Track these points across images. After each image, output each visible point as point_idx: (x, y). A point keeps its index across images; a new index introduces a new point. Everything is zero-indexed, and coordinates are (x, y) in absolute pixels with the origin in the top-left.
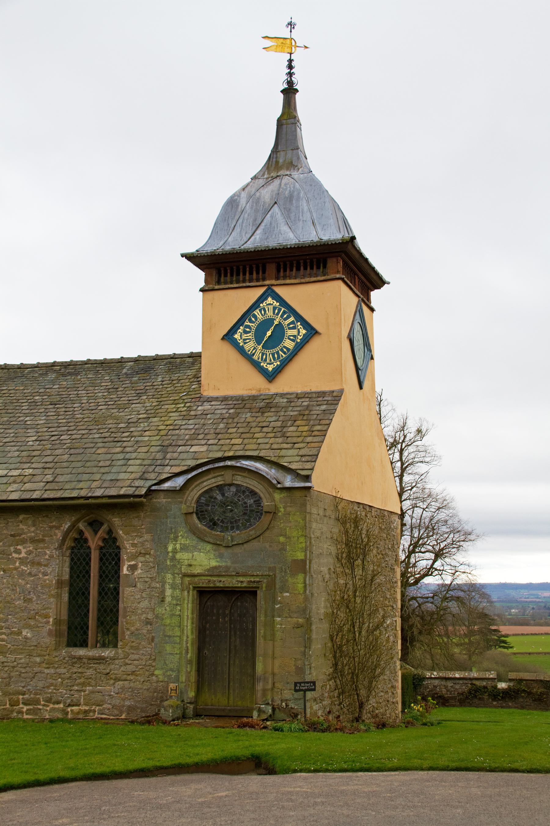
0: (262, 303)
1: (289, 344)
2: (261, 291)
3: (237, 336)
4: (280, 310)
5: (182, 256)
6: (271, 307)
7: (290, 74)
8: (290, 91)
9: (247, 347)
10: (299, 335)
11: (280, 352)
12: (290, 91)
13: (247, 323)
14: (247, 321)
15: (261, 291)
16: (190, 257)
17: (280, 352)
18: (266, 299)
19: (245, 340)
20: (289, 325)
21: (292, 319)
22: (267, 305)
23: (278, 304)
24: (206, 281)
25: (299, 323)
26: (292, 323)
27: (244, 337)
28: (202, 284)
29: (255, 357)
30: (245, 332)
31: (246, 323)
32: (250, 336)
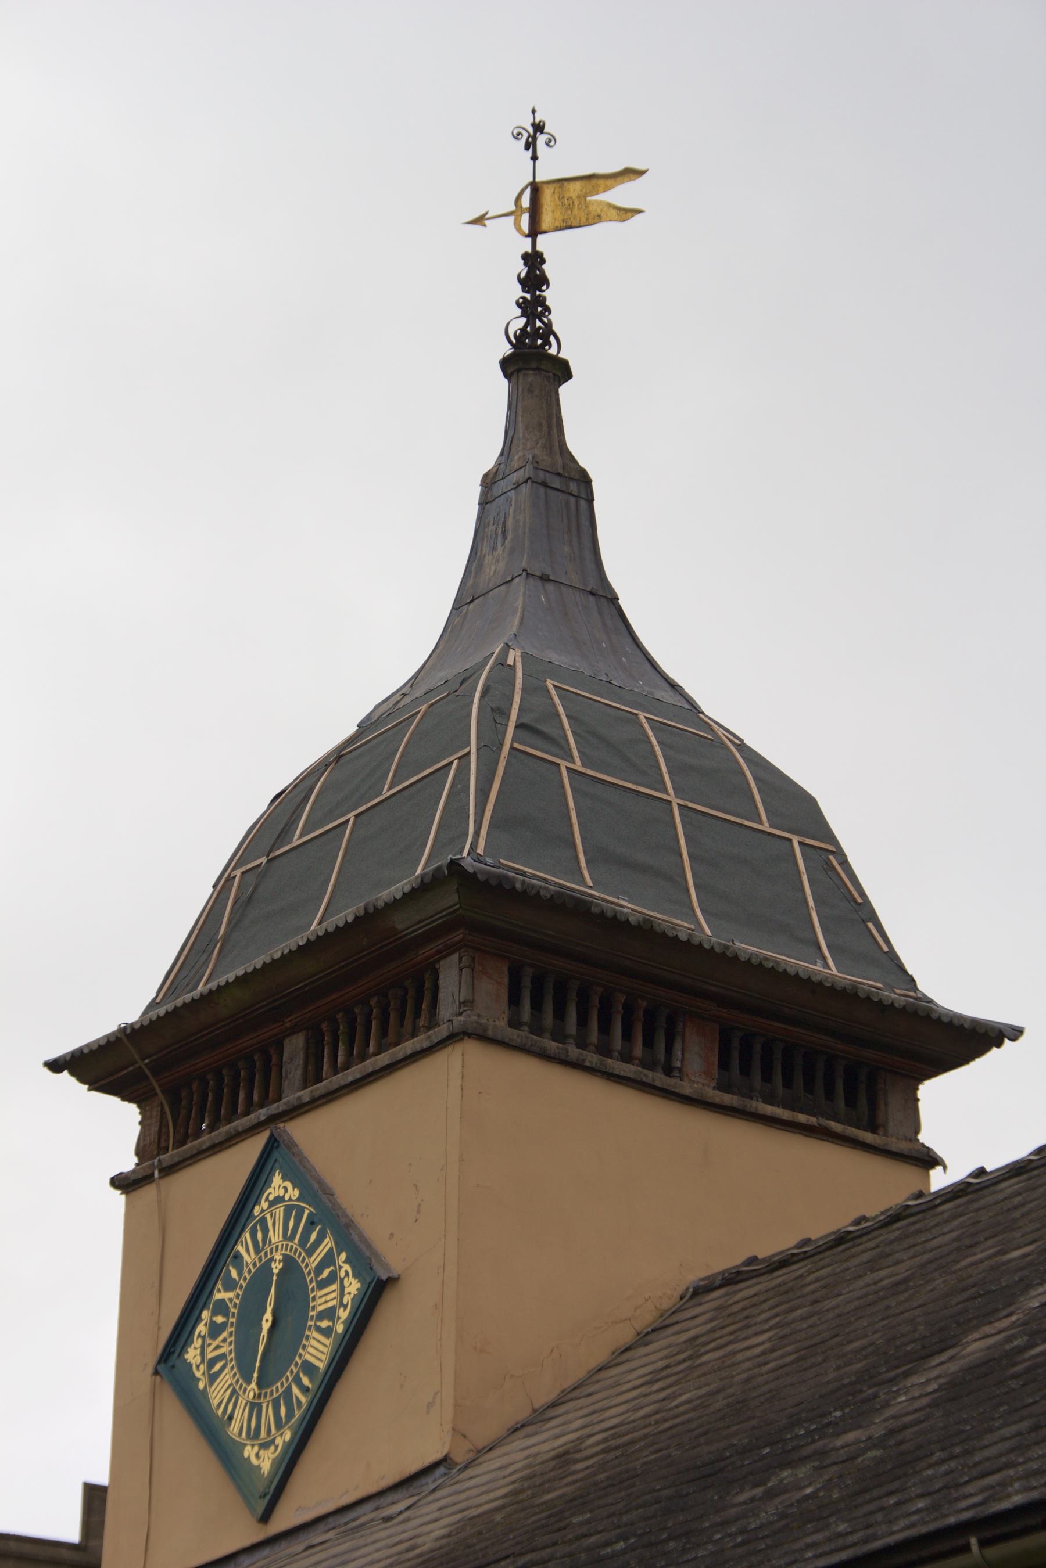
0: (257, 1202)
1: (317, 1350)
2: (252, 1148)
3: (192, 1355)
4: (301, 1211)
5: (55, 1066)
6: (280, 1211)
7: (533, 306)
8: (534, 364)
9: (217, 1395)
10: (341, 1304)
11: (296, 1390)
12: (534, 364)
13: (220, 1295)
14: (219, 1285)
15: (252, 1148)
16: (55, 1066)
17: (296, 1390)
18: (268, 1183)
19: (212, 1362)
20: (319, 1270)
21: (328, 1243)
22: (272, 1204)
23: (297, 1192)
24: (142, 1151)
25: (343, 1256)
26: (329, 1260)
27: (210, 1355)
28: (128, 1163)
29: (234, 1429)
30: (215, 1330)
31: (218, 1296)
32: (225, 1345)
